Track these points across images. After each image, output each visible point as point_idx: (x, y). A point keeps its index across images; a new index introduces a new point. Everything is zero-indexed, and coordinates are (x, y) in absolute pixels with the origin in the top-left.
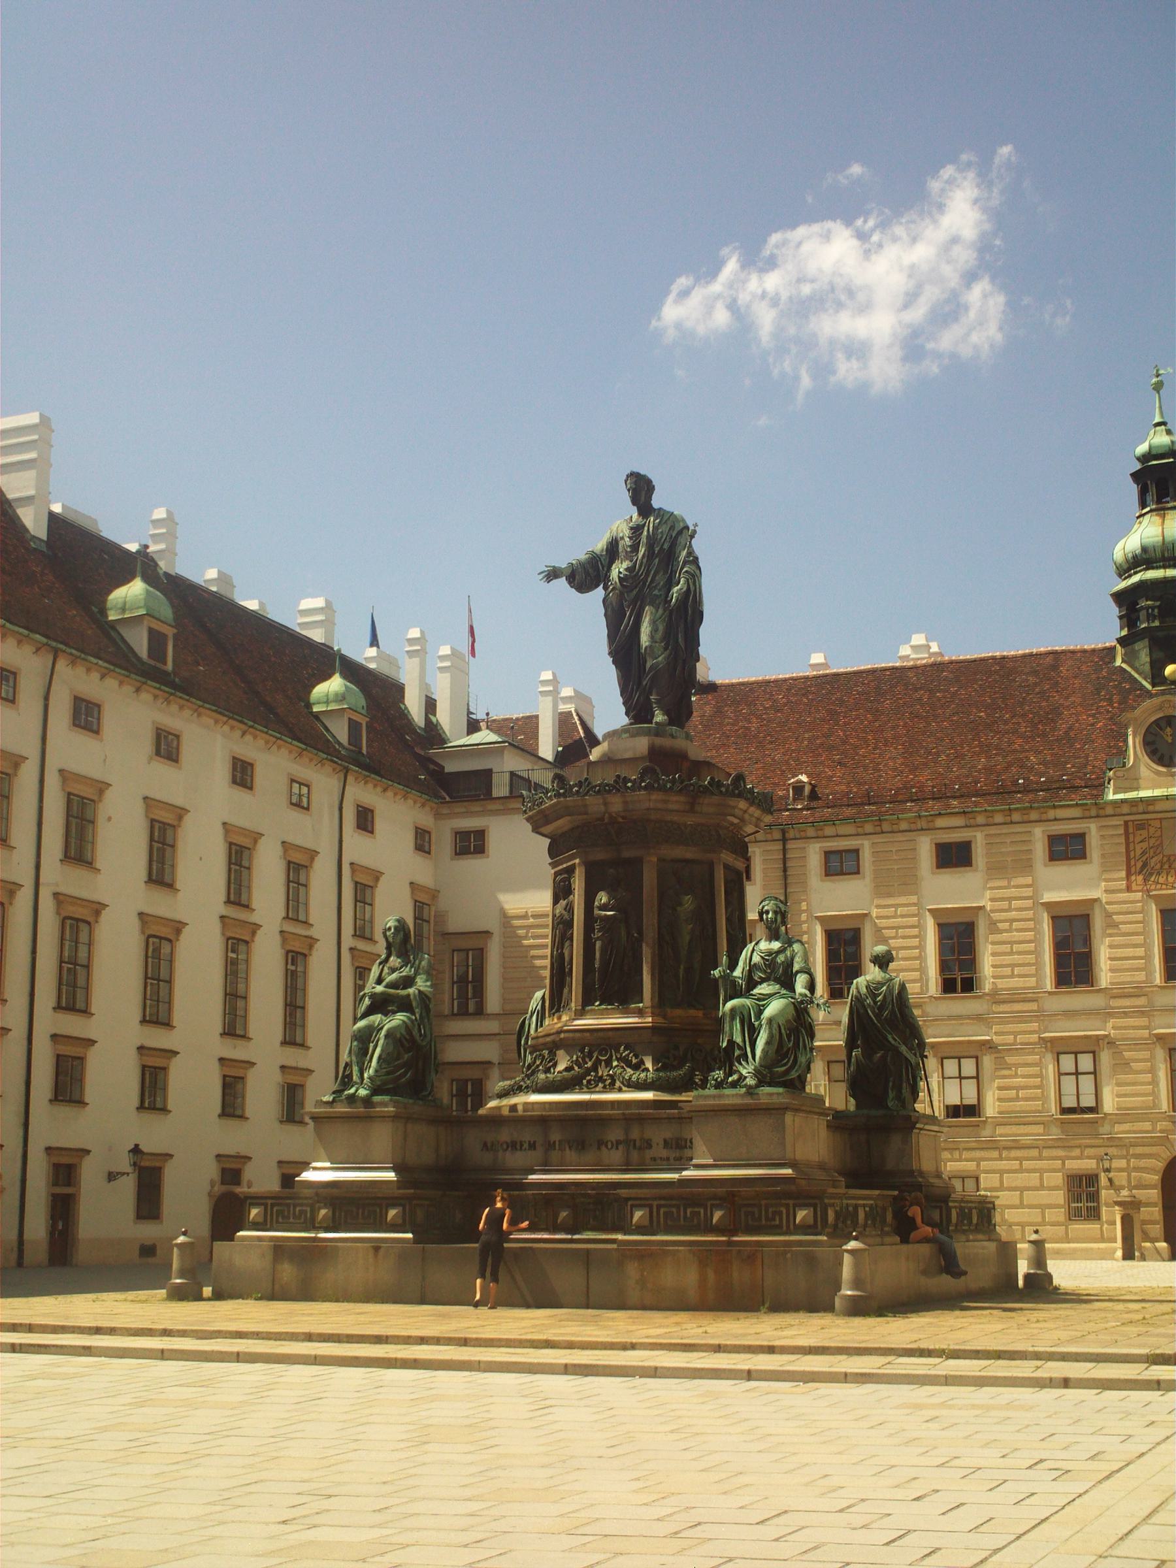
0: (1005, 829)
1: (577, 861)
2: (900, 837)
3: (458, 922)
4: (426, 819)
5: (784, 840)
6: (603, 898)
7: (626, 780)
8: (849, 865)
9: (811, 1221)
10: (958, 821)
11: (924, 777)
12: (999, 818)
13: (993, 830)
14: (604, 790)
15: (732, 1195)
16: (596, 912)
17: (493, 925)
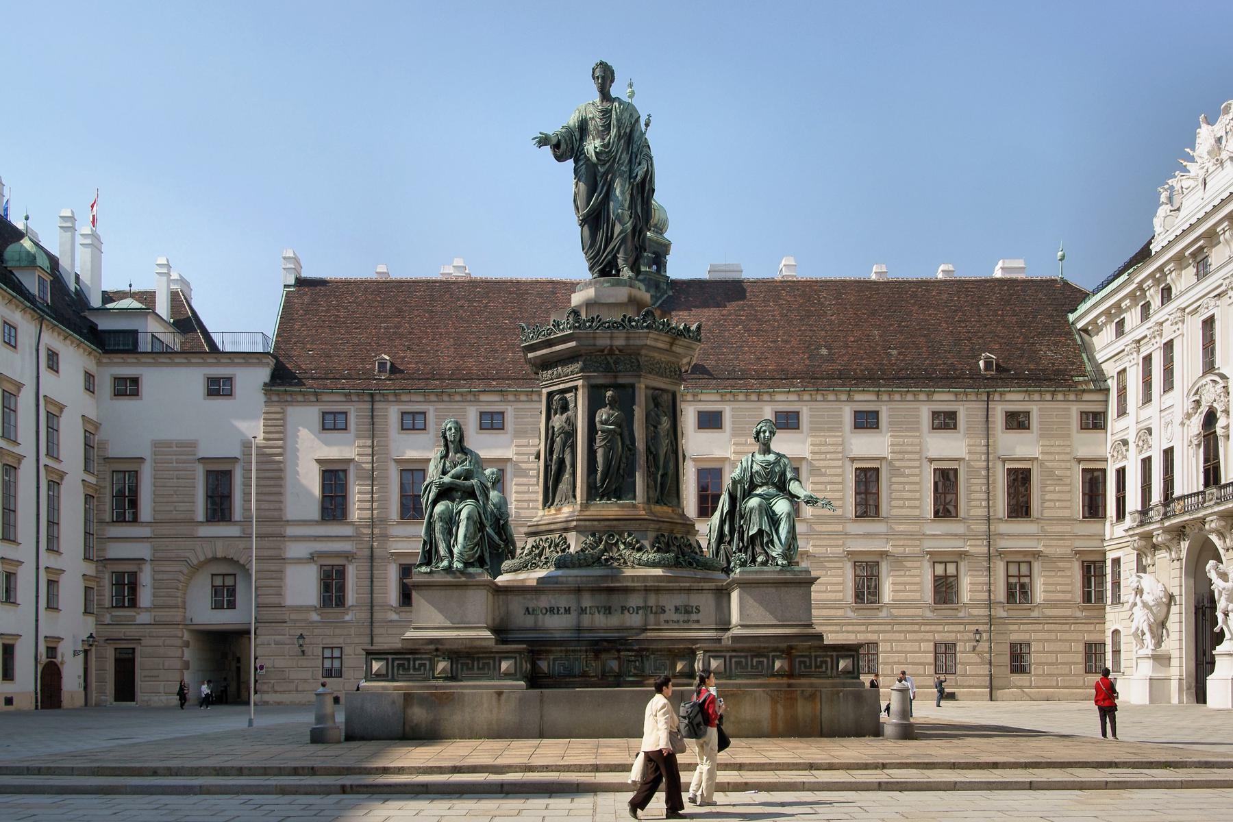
0: (528, 406)
1: (580, 383)
2: (456, 406)
3: (116, 450)
4: (92, 367)
5: (373, 402)
6: (602, 414)
7: (630, 320)
8: (419, 424)
9: (722, 669)
10: (496, 398)
11: (470, 362)
12: (523, 398)
13: (520, 405)
14: (613, 326)
15: (791, 648)
16: (598, 426)
17: (146, 452)
